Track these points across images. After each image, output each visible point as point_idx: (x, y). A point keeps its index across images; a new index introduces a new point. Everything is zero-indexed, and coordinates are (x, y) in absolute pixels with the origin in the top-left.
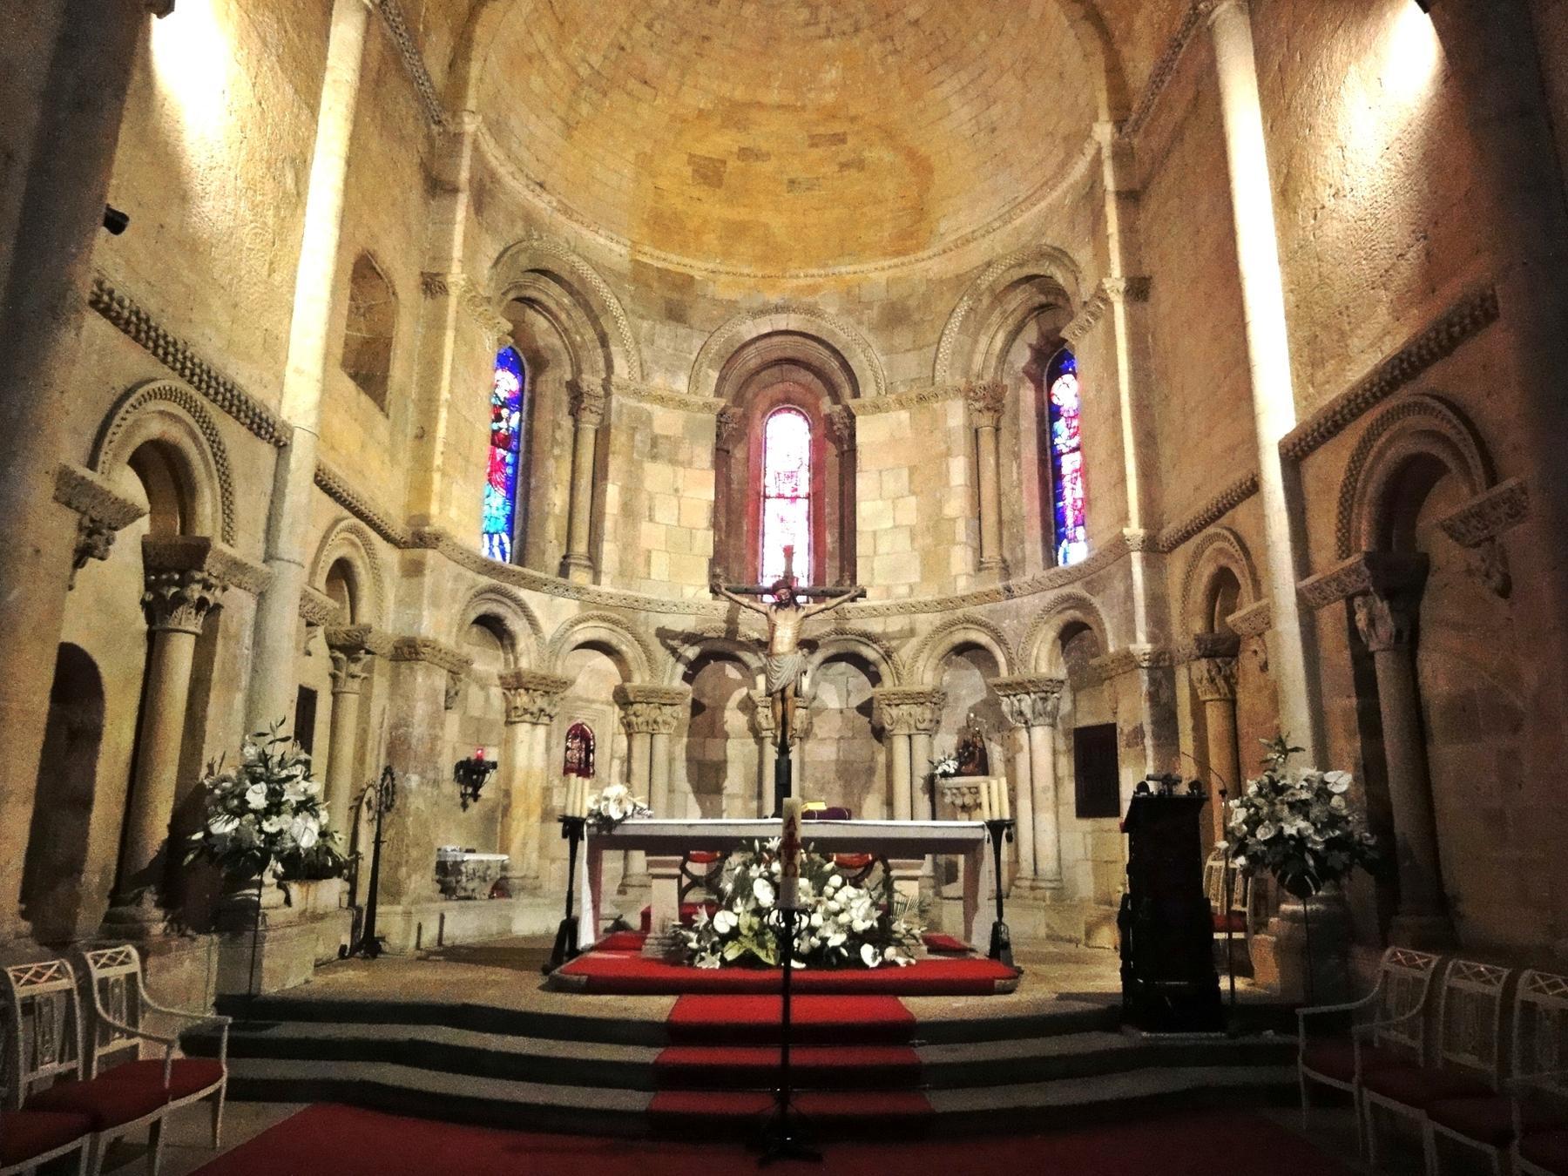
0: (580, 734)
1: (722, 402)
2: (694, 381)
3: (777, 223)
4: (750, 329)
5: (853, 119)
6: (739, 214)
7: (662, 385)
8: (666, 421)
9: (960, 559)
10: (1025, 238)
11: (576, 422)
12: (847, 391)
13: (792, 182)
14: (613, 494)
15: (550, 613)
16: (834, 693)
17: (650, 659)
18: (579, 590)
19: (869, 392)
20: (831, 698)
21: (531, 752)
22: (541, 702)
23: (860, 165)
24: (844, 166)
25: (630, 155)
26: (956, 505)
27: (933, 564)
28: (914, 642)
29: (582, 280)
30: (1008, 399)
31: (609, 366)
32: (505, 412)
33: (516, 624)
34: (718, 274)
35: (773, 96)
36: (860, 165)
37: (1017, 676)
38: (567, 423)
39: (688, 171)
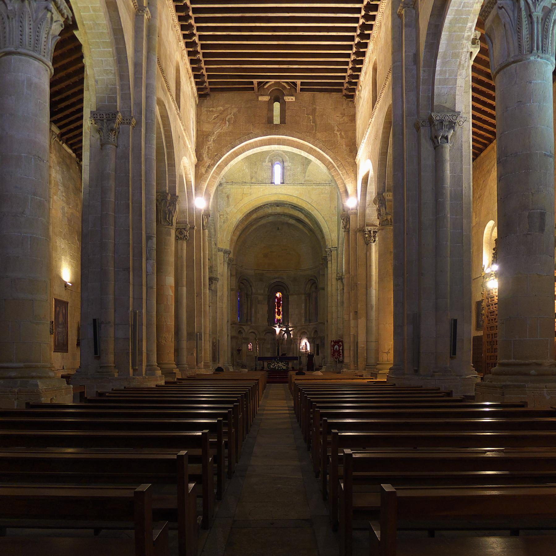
4: (272, 282)
8: (260, 298)
9: (303, 320)
15: (246, 328)
26: (303, 311)
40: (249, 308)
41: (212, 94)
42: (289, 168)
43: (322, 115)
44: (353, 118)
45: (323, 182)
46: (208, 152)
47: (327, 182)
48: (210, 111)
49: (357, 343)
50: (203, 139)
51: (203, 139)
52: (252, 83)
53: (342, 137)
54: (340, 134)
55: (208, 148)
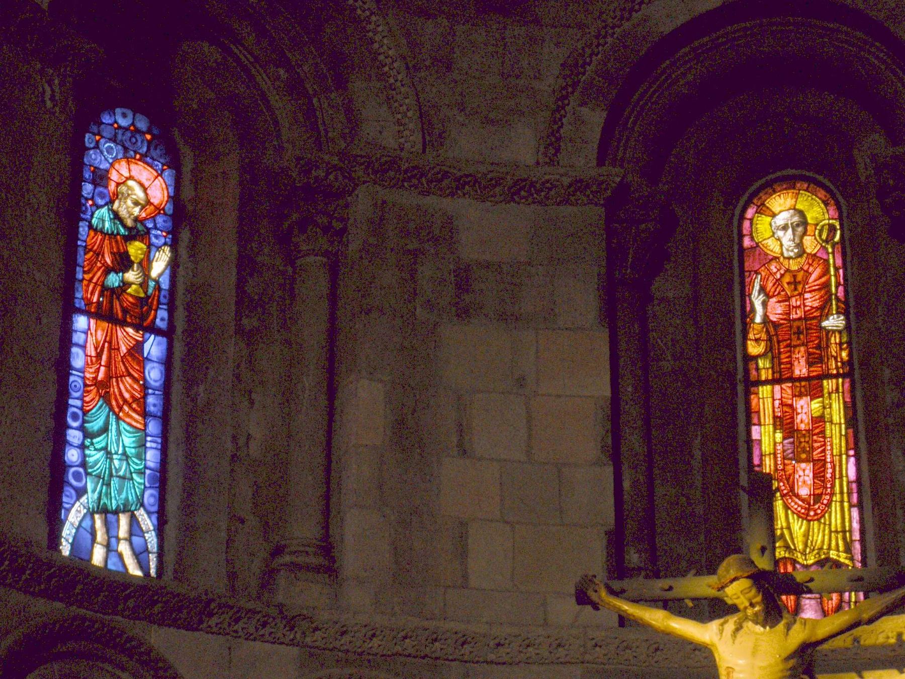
1: (614, 174)
2: (553, 143)
31: (353, 123)
32: (135, 249)
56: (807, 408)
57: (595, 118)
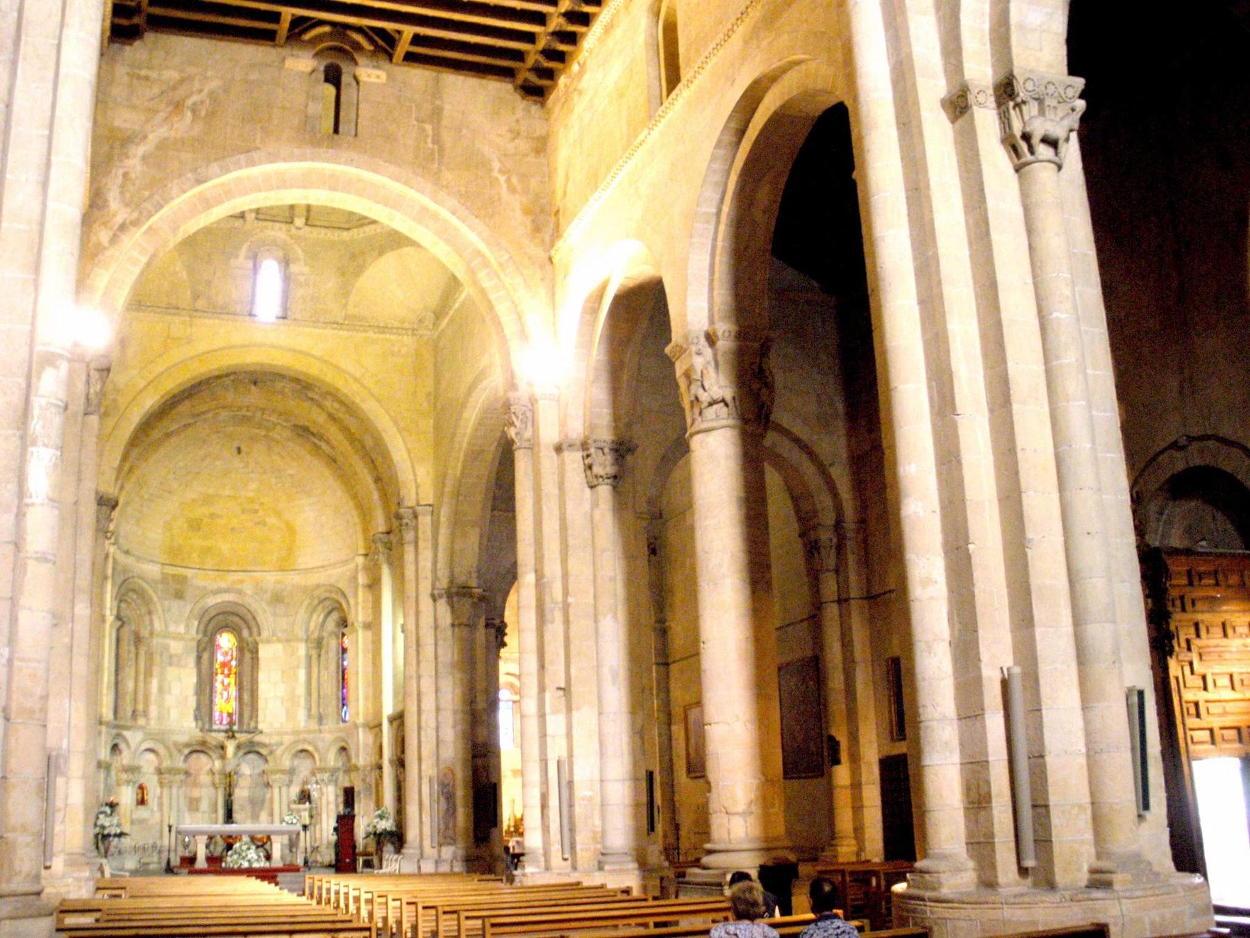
0: (141, 788)
1: (200, 636)
2: (187, 627)
3: (225, 547)
4: (212, 601)
5: (262, 504)
6: (208, 543)
7: (175, 629)
8: (176, 647)
9: (301, 714)
10: (332, 581)
11: (137, 649)
12: (255, 630)
13: (233, 529)
14: (155, 683)
16: (248, 768)
17: (171, 756)
18: (142, 728)
19: (265, 634)
20: (246, 769)
21: (126, 796)
22: (131, 777)
23: (265, 525)
24: (257, 524)
25: (161, 523)
26: (301, 690)
27: (291, 715)
28: (282, 748)
29: (143, 590)
30: (325, 642)
33: (122, 746)
34: (199, 580)
35: (227, 492)
36: (265, 525)
37: (323, 765)
38: (133, 649)
39: (186, 526)
40: (141, 677)
41: (150, 37)
42: (302, 279)
43: (459, 130)
44: (542, 146)
45: (396, 324)
46: (122, 186)
47: (406, 325)
48: (139, 77)
49: (570, 783)
50: (112, 147)
51: (112, 147)
52: (276, 17)
53: (512, 190)
54: (508, 180)
55: (125, 175)
56: (227, 681)
57: (196, 623)
